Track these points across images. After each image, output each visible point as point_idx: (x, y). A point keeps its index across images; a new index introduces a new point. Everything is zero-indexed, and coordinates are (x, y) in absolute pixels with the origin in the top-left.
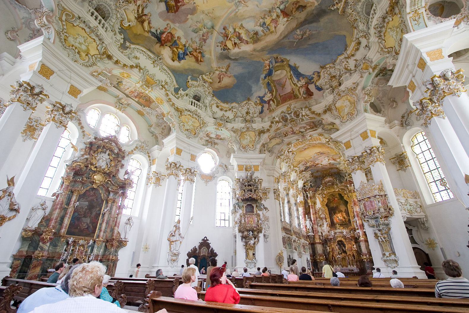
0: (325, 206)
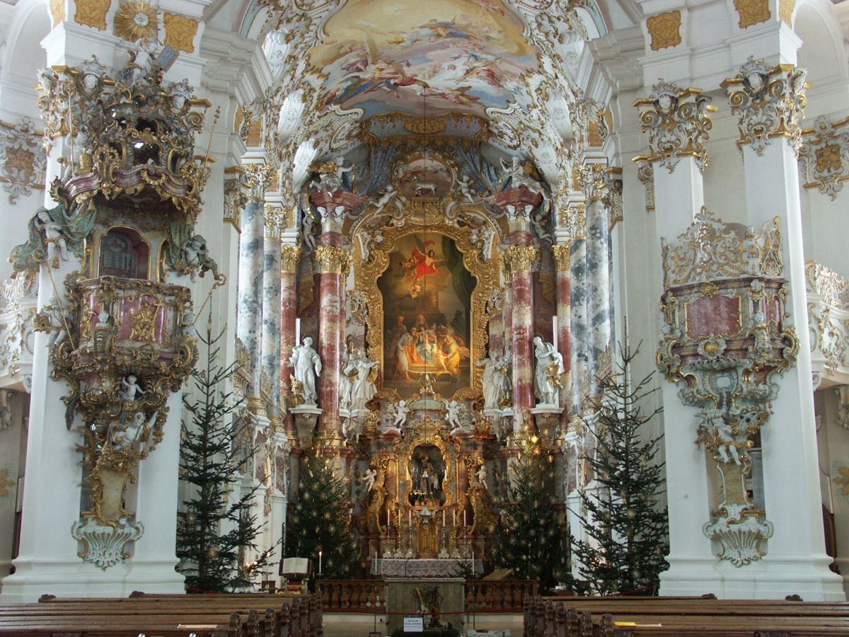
0: (375, 288)
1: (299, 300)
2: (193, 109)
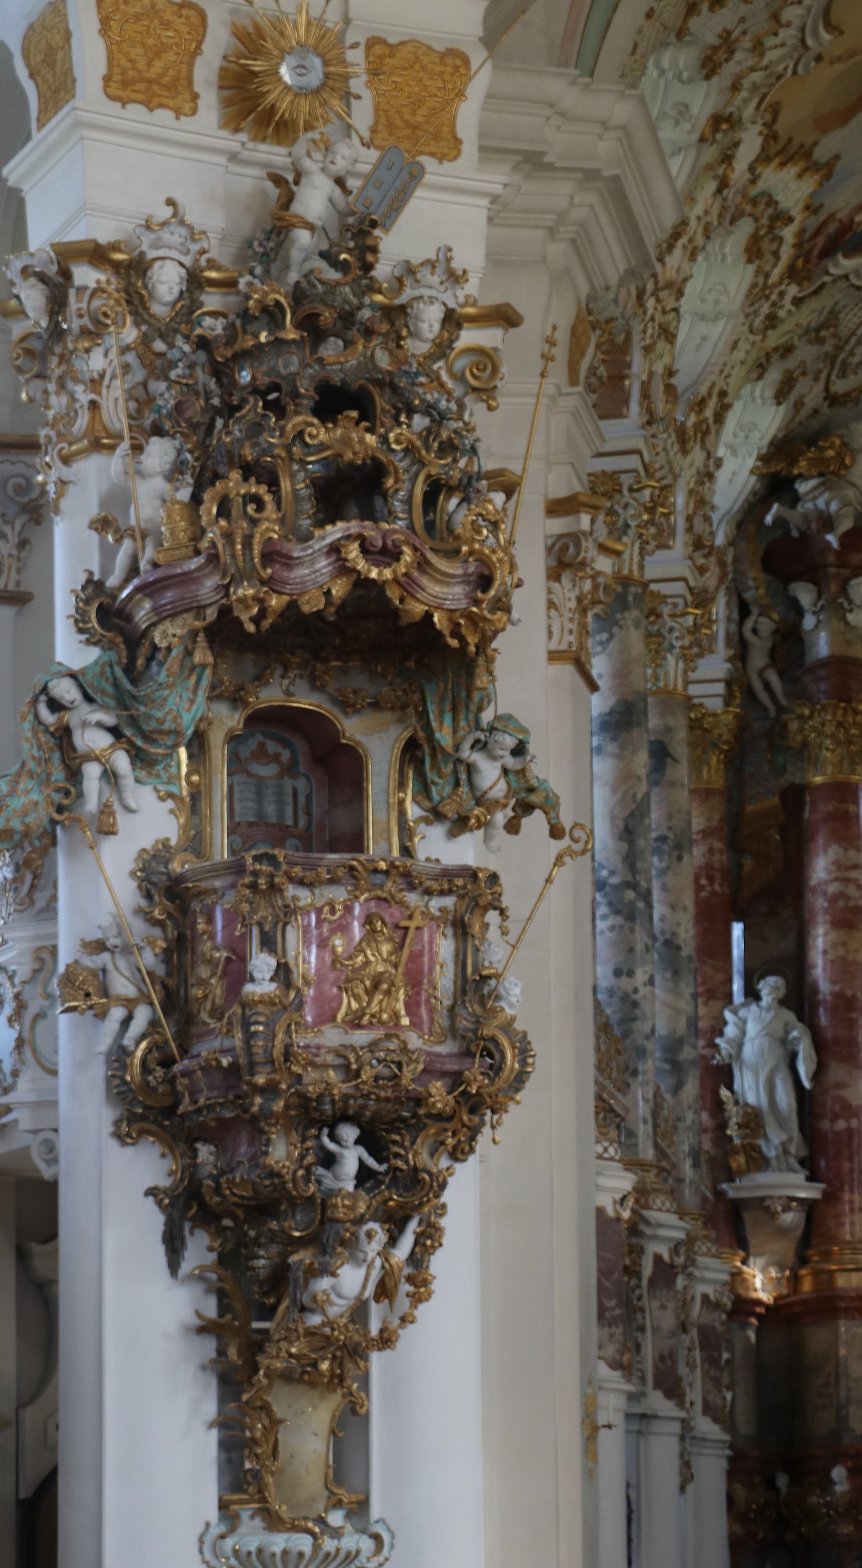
1: (740, 866)
2: (468, 337)
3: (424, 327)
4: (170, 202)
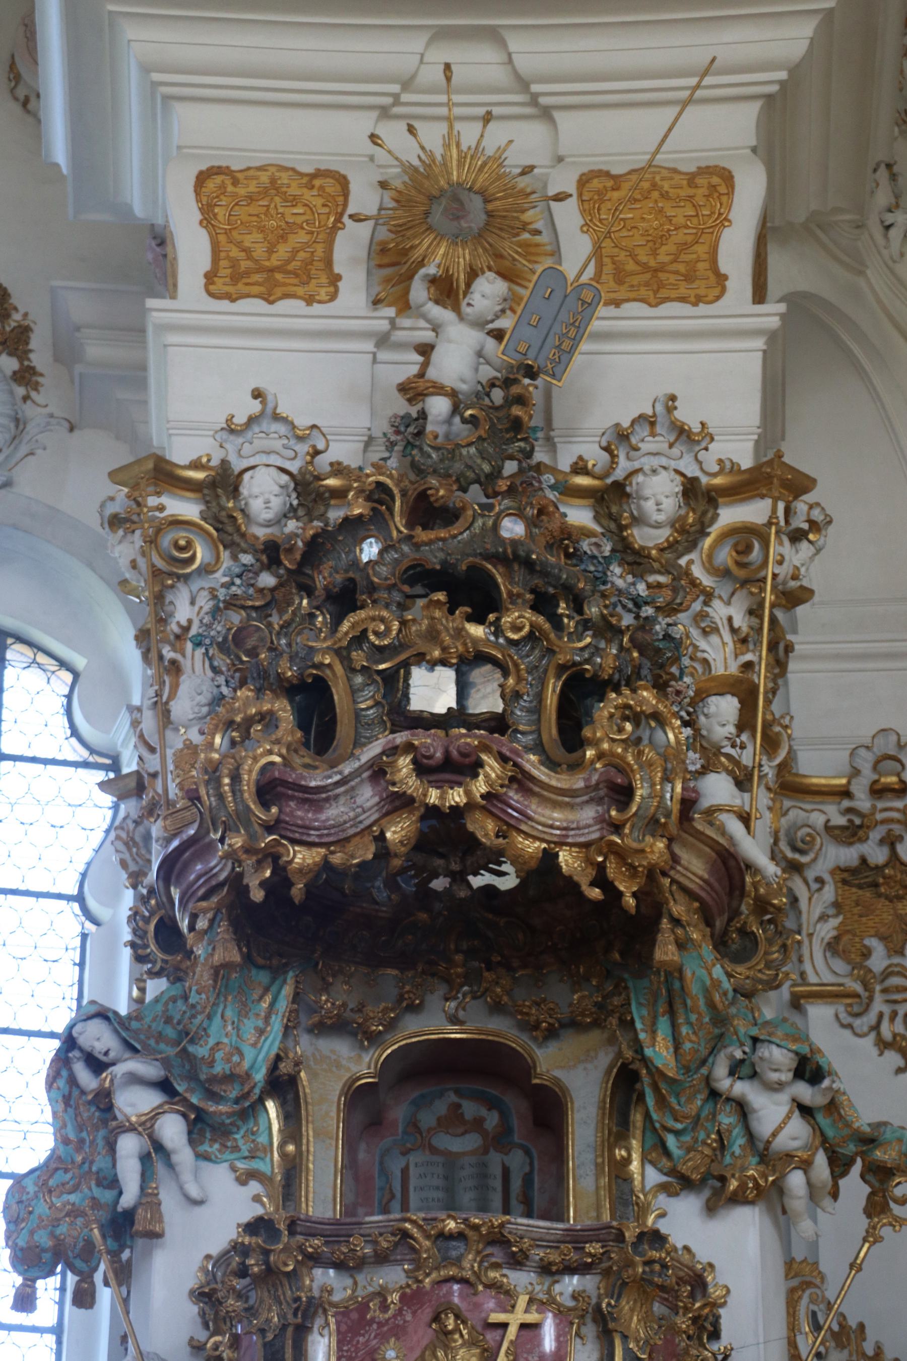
3: (649, 506)
4: (257, 394)
